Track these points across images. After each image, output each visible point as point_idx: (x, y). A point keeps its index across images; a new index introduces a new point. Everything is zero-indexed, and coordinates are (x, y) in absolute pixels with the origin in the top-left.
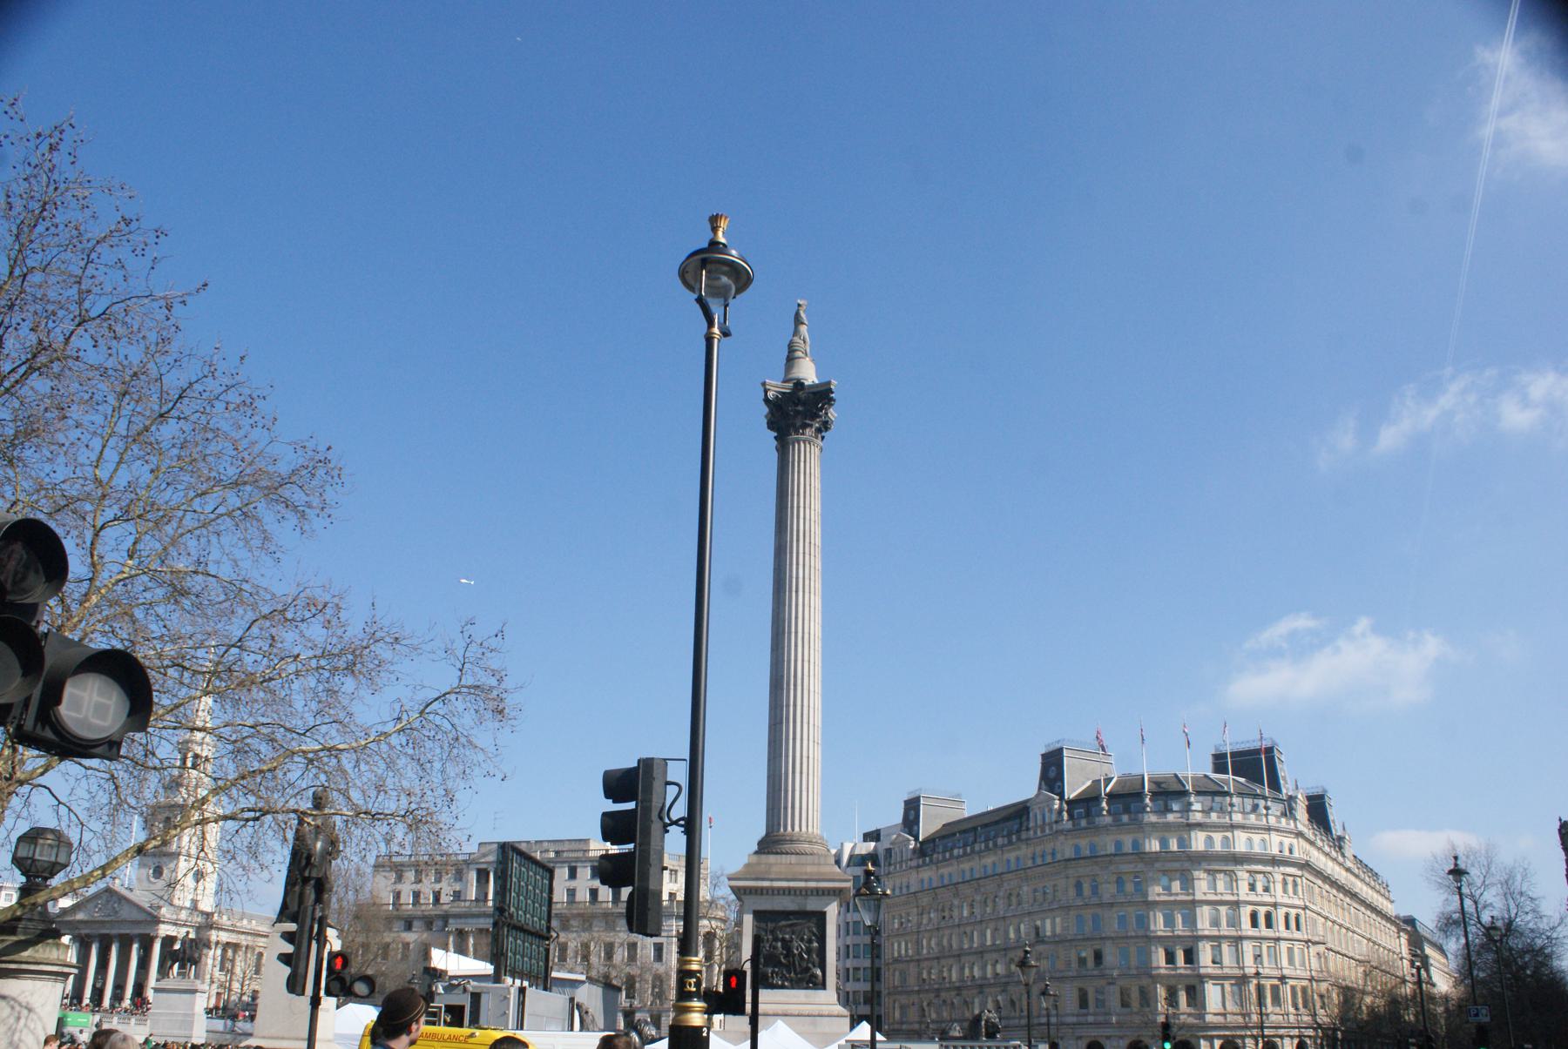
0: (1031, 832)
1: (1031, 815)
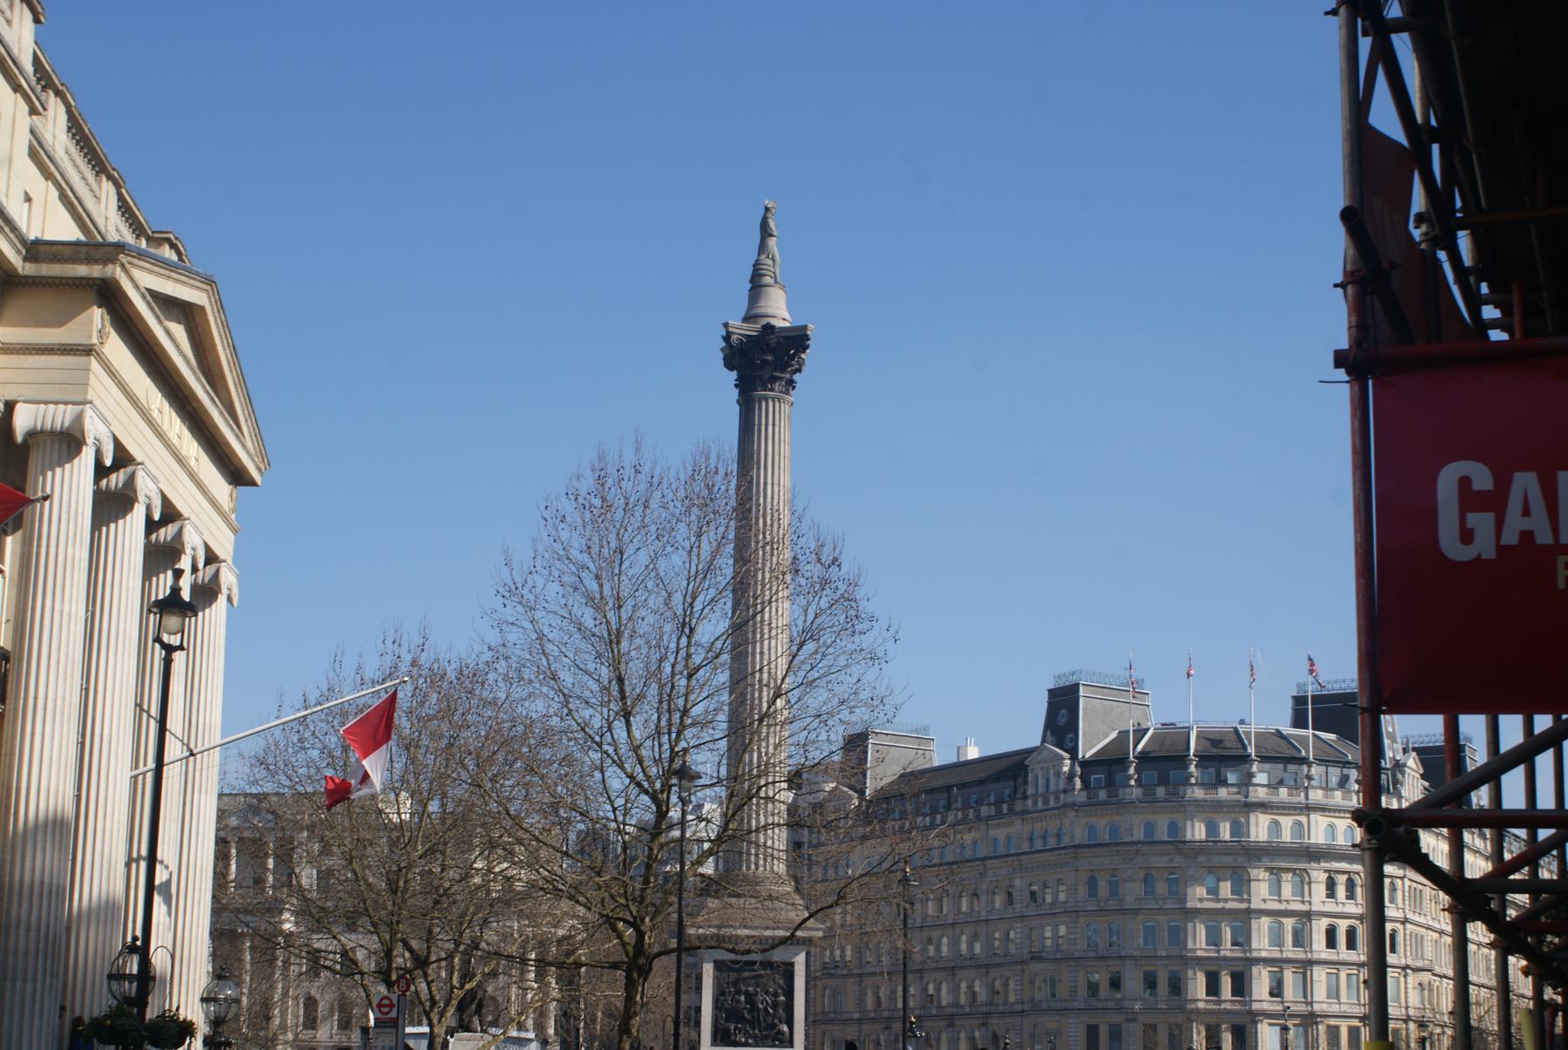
0: (1030, 802)
1: (1030, 779)
